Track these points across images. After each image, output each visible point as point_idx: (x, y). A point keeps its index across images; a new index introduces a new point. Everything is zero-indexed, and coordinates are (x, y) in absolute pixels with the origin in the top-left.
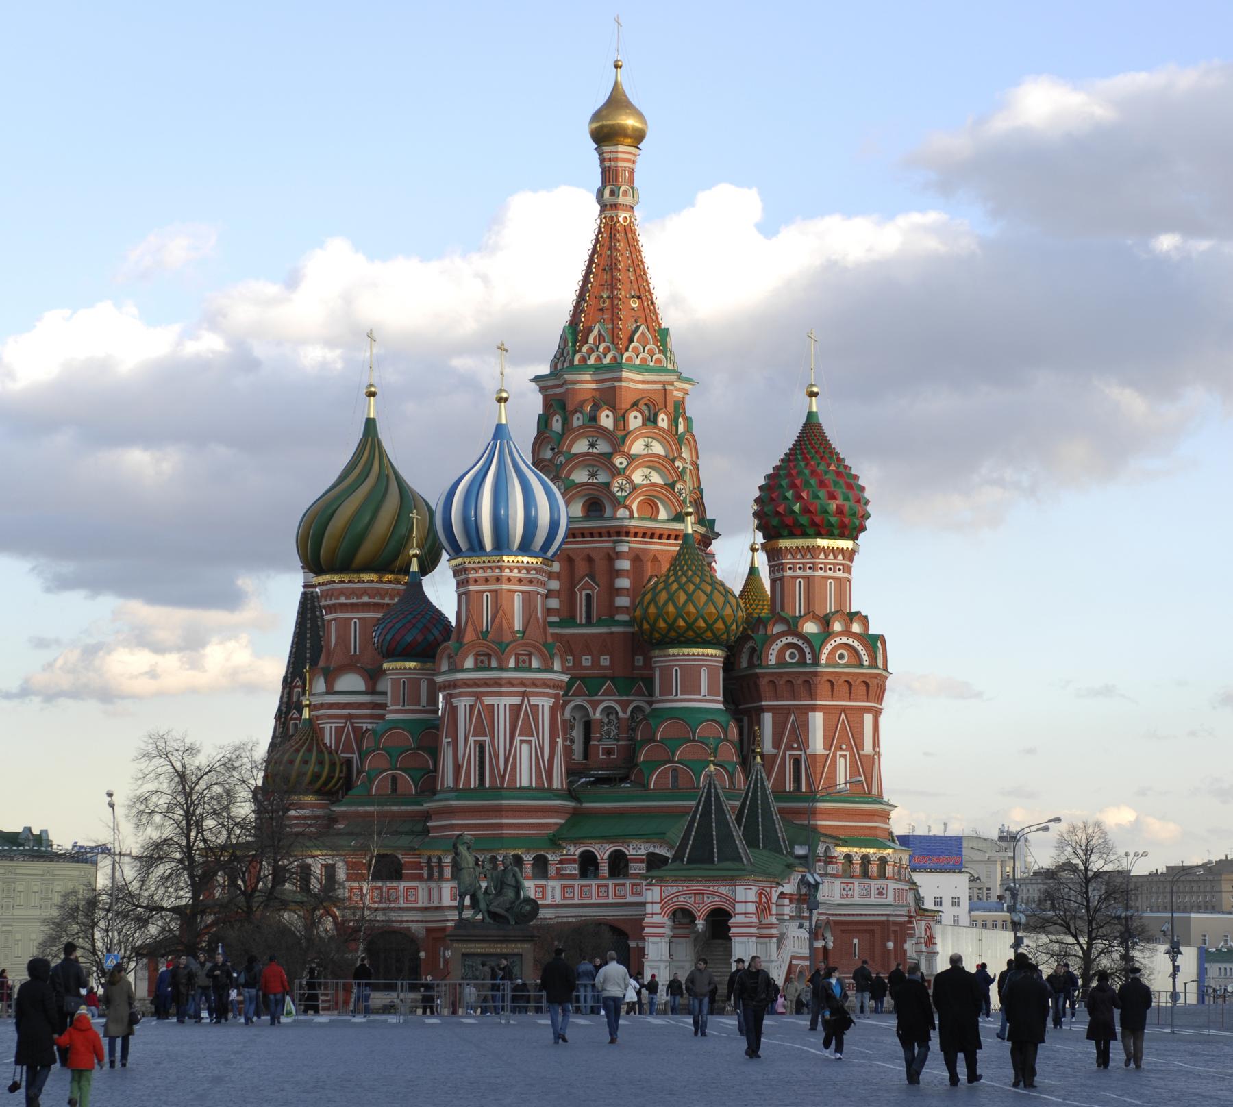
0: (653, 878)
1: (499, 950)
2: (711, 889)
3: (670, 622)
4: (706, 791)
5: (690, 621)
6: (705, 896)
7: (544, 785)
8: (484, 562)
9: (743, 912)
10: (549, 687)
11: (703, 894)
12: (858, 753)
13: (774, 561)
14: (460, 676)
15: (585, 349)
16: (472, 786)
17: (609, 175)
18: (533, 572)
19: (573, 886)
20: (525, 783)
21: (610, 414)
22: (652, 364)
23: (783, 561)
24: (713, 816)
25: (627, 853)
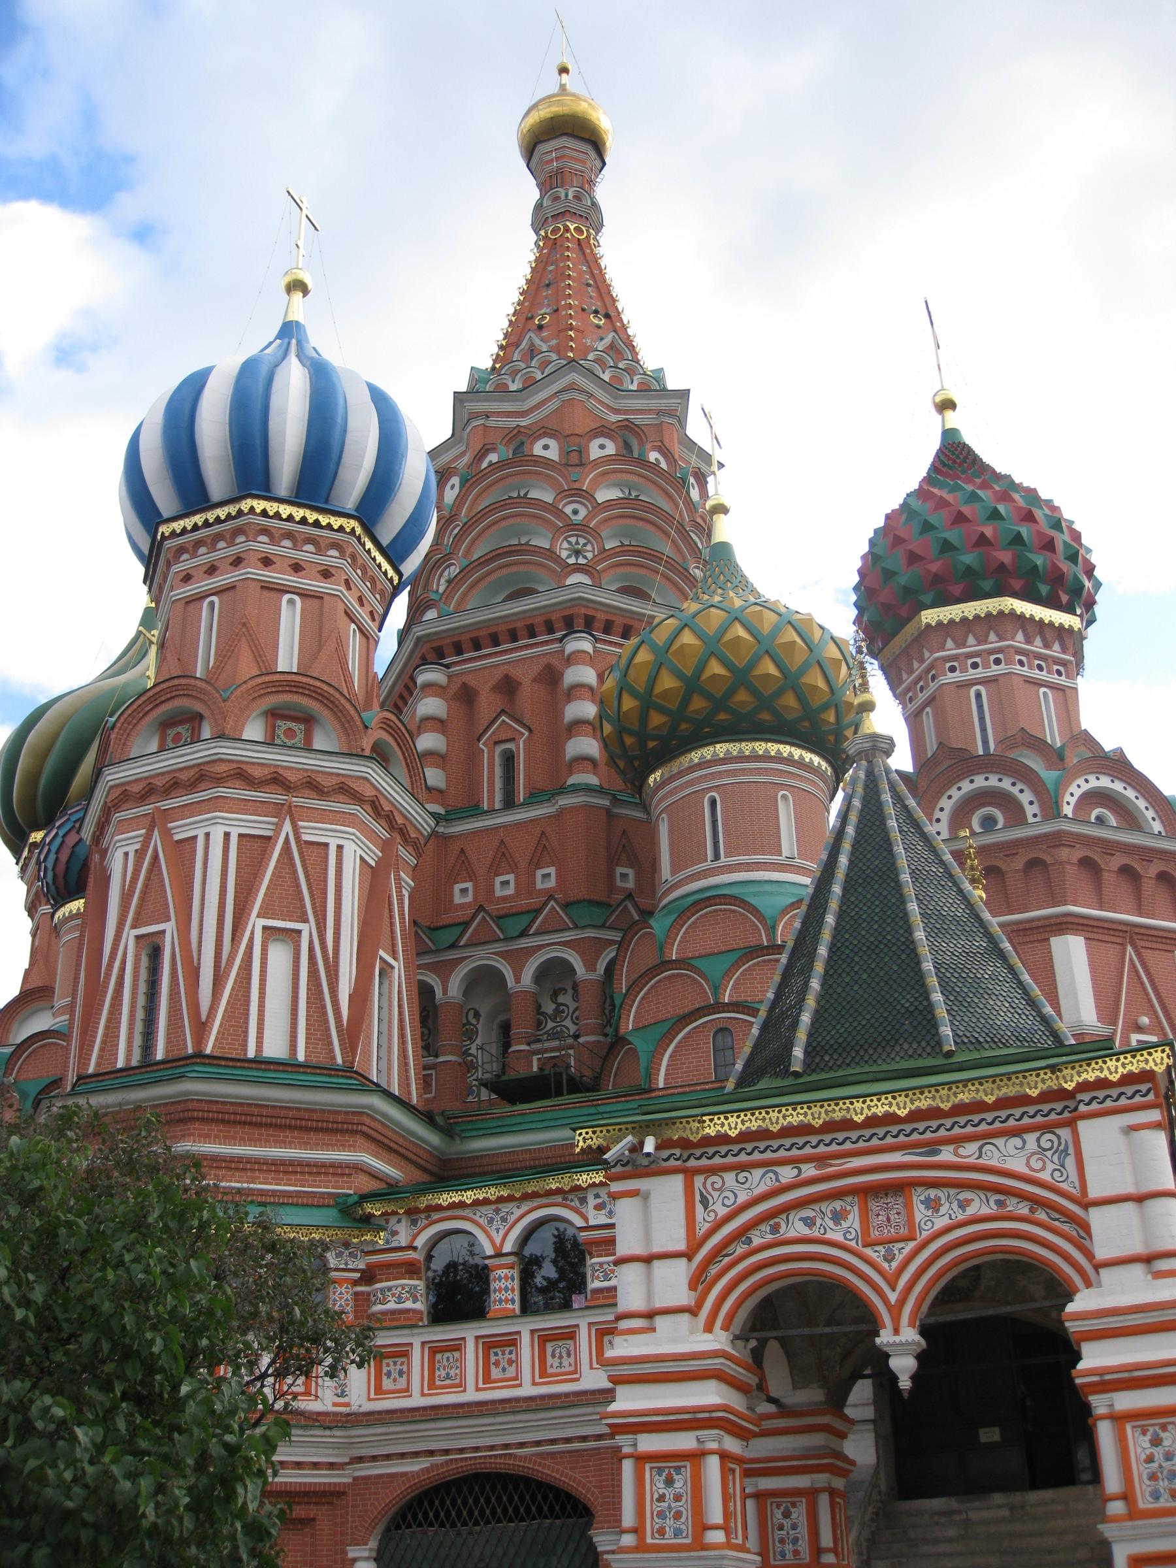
0: (643, 1129)
2: (946, 1155)
3: (689, 674)
5: (740, 662)
6: (918, 1196)
7: (334, 1058)
8: (206, 521)
9: (1137, 1247)
10: (356, 797)
11: (899, 1188)
14: (113, 776)
16: (120, 1064)
17: (549, 182)
19: (403, 1353)
20: (275, 1048)
21: (553, 443)
22: (634, 387)
23: (937, 655)
24: (905, 877)
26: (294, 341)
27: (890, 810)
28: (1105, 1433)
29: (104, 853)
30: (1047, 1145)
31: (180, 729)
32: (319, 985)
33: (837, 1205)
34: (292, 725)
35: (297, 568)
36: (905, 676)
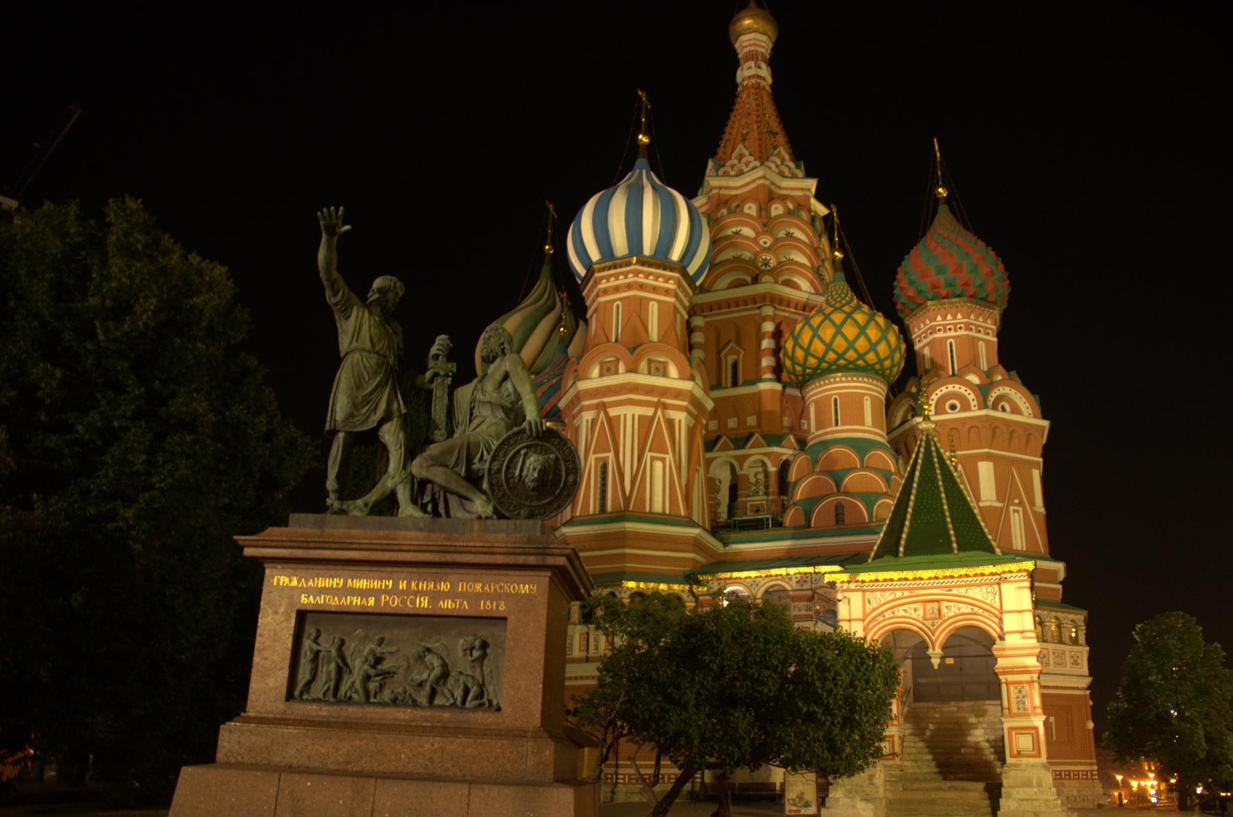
1: (423, 603)
2: (955, 591)
4: (922, 450)
6: (944, 604)
11: (938, 601)
12: (1031, 509)
13: (919, 329)
14: (583, 385)
15: (729, 163)
16: (591, 512)
18: (671, 281)
20: (658, 508)
22: (790, 175)
23: (933, 323)
24: (940, 483)
25: (788, 588)
26: (644, 171)
27: (934, 454)
28: (1004, 687)
29: (574, 417)
30: (989, 590)
31: (609, 365)
32: (674, 481)
33: (915, 605)
34: (658, 365)
35: (655, 289)
36: (916, 330)
